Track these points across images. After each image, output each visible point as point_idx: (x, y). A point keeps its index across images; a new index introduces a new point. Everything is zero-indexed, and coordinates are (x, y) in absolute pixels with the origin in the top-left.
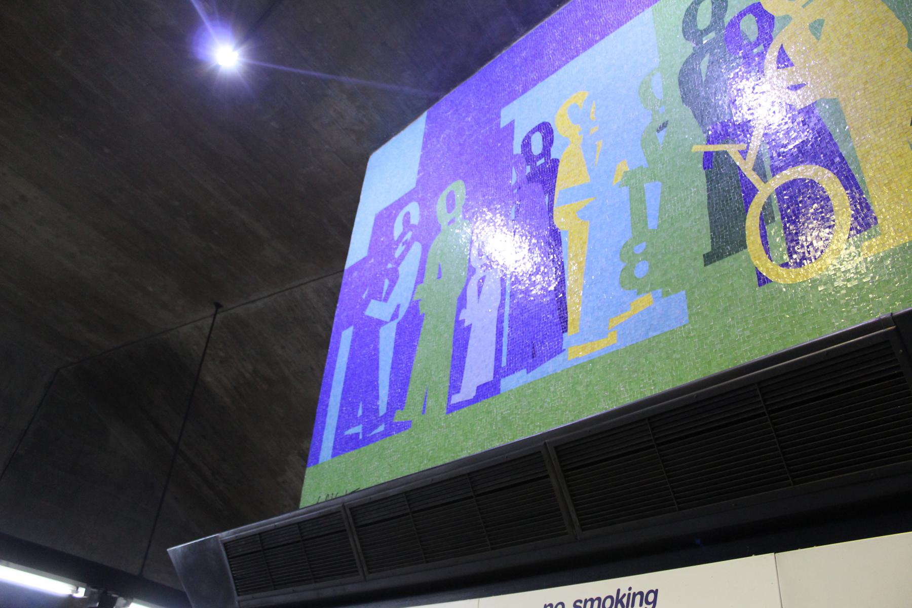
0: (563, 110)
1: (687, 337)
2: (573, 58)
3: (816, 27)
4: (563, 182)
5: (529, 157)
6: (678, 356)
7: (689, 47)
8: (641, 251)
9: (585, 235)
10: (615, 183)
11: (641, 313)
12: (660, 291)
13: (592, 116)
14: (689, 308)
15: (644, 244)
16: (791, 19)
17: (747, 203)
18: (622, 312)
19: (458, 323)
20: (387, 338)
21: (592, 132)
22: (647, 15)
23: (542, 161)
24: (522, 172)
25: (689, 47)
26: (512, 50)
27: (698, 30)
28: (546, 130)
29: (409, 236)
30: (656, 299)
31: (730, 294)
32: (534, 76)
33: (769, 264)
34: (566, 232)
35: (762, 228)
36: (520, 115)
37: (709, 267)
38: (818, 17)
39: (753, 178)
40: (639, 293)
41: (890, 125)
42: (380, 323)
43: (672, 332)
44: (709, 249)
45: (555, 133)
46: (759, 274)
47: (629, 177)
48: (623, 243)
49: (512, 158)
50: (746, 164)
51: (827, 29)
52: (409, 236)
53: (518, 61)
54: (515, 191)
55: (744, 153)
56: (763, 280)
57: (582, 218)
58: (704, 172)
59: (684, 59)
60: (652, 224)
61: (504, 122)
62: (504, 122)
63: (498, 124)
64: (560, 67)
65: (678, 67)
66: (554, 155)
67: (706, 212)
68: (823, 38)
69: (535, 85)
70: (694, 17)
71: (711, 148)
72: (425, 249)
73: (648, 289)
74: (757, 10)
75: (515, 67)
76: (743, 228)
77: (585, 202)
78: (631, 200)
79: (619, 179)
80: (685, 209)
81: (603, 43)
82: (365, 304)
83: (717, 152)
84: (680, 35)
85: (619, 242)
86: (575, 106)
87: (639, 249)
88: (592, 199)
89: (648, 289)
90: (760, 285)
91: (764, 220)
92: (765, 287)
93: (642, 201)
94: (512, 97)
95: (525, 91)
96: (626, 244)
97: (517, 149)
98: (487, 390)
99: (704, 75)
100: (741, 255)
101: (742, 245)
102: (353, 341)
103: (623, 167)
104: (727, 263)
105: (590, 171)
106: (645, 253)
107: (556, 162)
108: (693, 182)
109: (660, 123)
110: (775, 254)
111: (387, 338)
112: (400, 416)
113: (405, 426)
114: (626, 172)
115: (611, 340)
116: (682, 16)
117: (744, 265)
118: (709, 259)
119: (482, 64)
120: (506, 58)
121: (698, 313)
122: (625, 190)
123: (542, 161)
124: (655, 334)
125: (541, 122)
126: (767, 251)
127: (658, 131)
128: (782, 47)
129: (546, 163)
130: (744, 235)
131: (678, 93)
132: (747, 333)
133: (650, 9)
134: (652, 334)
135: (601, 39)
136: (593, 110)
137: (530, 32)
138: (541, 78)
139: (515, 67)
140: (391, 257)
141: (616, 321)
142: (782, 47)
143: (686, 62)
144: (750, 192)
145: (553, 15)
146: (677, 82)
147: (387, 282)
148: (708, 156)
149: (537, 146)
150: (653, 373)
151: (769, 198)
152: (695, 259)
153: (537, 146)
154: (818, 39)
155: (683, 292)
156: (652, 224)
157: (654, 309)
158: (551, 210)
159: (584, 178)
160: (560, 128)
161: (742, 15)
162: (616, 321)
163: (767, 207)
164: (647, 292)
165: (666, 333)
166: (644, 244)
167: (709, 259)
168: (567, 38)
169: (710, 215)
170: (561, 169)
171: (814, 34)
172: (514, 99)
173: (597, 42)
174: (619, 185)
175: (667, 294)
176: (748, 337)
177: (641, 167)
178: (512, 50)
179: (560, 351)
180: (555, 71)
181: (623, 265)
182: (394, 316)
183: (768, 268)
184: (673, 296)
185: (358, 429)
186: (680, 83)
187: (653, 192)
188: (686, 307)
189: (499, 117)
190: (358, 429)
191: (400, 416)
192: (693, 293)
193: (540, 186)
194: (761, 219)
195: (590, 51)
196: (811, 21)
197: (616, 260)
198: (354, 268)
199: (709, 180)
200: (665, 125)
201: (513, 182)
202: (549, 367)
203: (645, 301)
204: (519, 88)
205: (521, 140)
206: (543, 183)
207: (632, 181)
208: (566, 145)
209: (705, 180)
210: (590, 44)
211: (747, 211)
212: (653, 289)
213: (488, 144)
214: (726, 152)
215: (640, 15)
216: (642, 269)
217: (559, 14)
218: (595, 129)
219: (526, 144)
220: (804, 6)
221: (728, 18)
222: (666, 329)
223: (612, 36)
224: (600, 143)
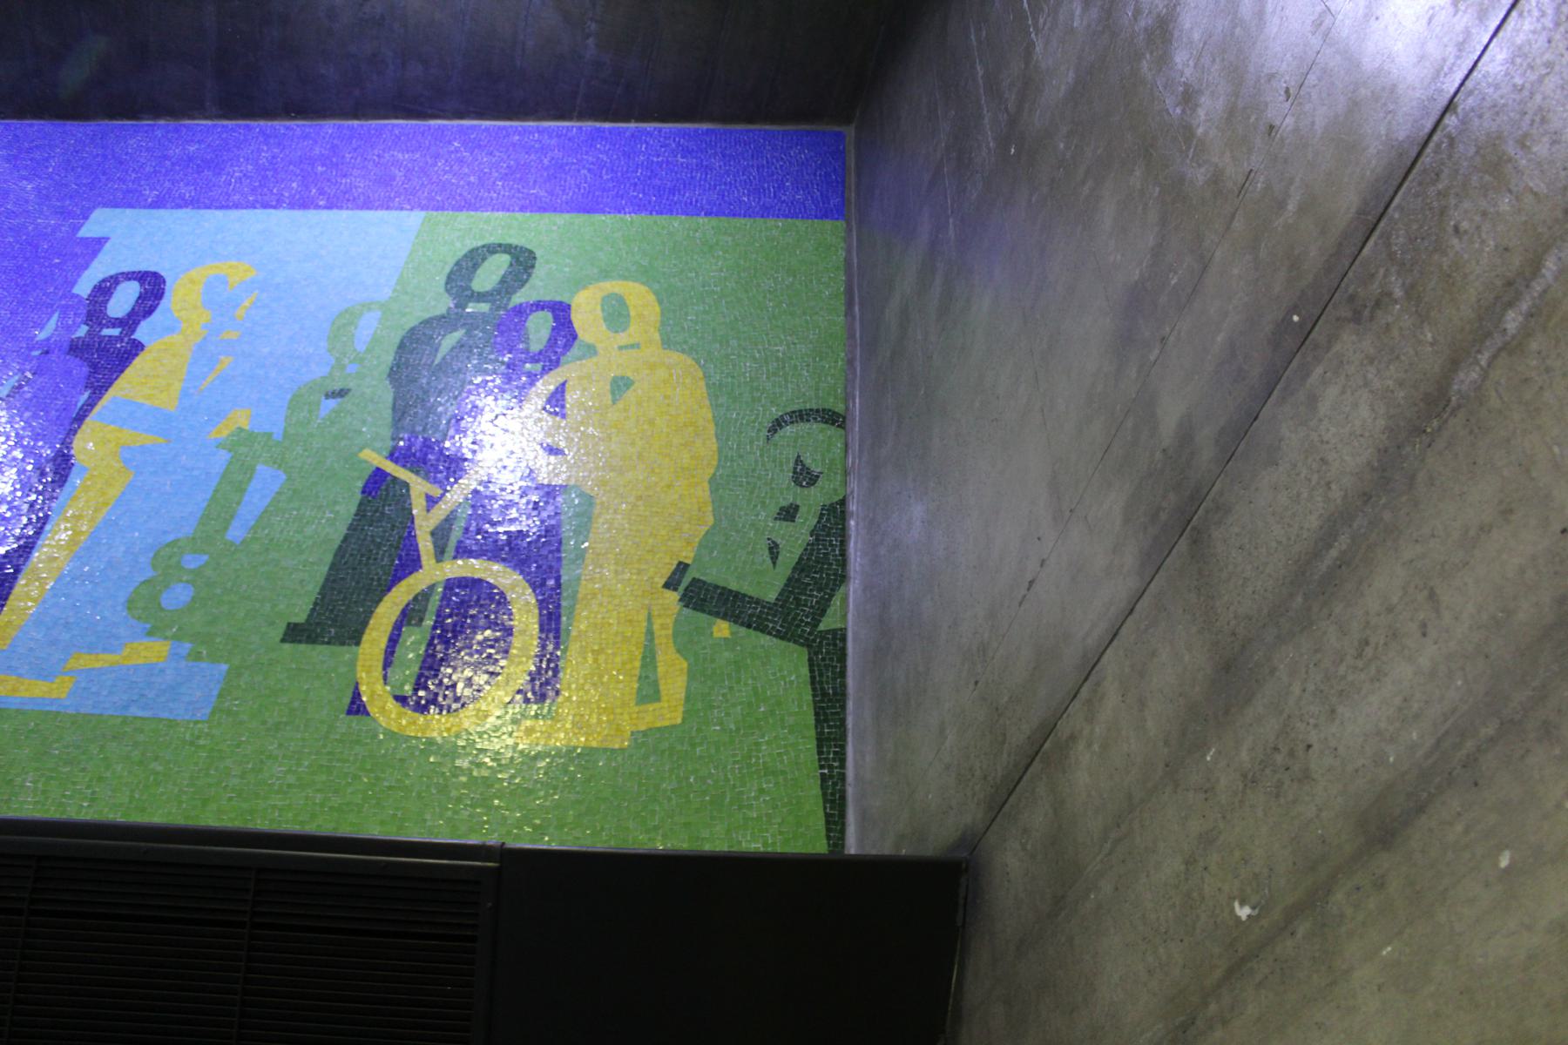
0: (200, 274)
1: (192, 743)
2: (266, 206)
3: (620, 385)
4: (129, 385)
6: (160, 768)
7: (443, 304)
8: (192, 567)
9: (114, 493)
10: (213, 435)
11: (136, 668)
12: (188, 645)
13: (240, 312)
14: (220, 696)
15: (205, 558)
16: (596, 353)
17: (396, 579)
18: (105, 650)
21: (225, 336)
22: (414, 219)
23: (116, 332)
24: (68, 329)
25: (443, 304)
26: (177, 130)
27: (469, 288)
28: (153, 288)
30: (174, 655)
31: (296, 704)
32: (187, 192)
33: (379, 687)
34: (85, 469)
35: (398, 627)
36: (126, 237)
37: (287, 646)
38: (629, 374)
39: (425, 545)
40: (150, 634)
41: (639, 572)
43: (172, 724)
44: (300, 617)
45: (164, 303)
46: (357, 695)
47: (243, 439)
48: (171, 537)
49: (64, 296)
50: (426, 519)
51: (630, 396)
53: (175, 151)
54: (36, 353)
55: (431, 501)
56: (357, 707)
57: (126, 462)
58: (359, 496)
59: (427, 316)
60: (236, 533)
61: (89, 230)
62: (89, 230)
63: (77, 228)
64: (237, 206)
65: (411, 322)
66: (140, 334)
67: (329, 558)
68: (620, 405)
69: (179, 207)
70: (476, 266)
71: (390, 467)
73: (169, 634)
74: (561, 312)
75: (166, 157)
76: (369, 613)
77: (147, 439)
78: (224, 476)
79: (223, 431)
80: (299, 537)
81: (325, 215)
83: (395, 478)
84: (441, 279)
85: (165, 532)
86: (223, 280)
87: (192, 562)
88: (161, 440)
89: (169, 634)
90: (349, 712)
91: (409, 616)
92: (355, 720)
93: (241, 490)
94: (129, 200)
95: (158, 204)
96: (176, 541)
97: (84, 287)
99: (439, 356)
100: (345, 653)
101: (356, 638)
103: (241, 419)
104: (318, 654)
105: (185, 394)
106: (198, 572)
107: (138, 347)
108: (335, 503)
109: (337, 386)
110: (395, 674)
114: (241, 430)
115: (55, 690)
116: (460, 254)
117: (342, 670)
118: (294, 633)
119: (112, 117)
120: (159, 133)
121: (229, 712)
122: (223, 456)
123: (116, 332)
124: (140, 713)
125: (152, 269)
126: (387, 664)
127: (327, 396)
128: (563, 384)
129: (119, 339)
130: (365, 623)
131: (389, 358)
132: (291, 779)
133: (423, 214)
134: (135, 711)
135: (329, 207)
136: (247, 303)
137: (225, 122)
138: (194, 203)
139: (166, 157)
141: (85, 661)
142: (563, 384)
143: (427, 322)
144: (411, 563)
145: (275, 123)
146: (397, 341)
148: (379, 476)
149: (122, 301)
150: (100, 779)
151: (432, 587)
152: (273, 623)
153: (122, 301)
154: (614, 402)
155: (225, 667)
156: (236, 533)
157: (162, 671)
158: (80, 418)
159: (168, 401)
160: (177, 297)
161: (539, 306)
162: (85, 661)
163: (422, 598)
164: (166, 638)
165: (161, 720)
166: (205, 558)
167: (294, 633)
168: (275, 170)
169: (333, 566)
170: (137, 361)
171: (613, 393)
172: (131, 206)
173: (318, 207)
174: (220, 445)
175: (198, 657)
176: (289, 786)
177: (270, 435)
178: (177, 130)
180: (227, 207)
181: (149, 574)
183: (375, 692)
184: (203, 665)
186: (401, 346)
187: (266, 483)
188: (215, 693)
189: (86, 218)
192: (239, 675)
193: (86, 370)
194: (404, 613)
195: (298, 214)
196: (619, 373)
197: (142, 559)
199: (361, 513)
200: (342, 393)
201: (41, 335)
203: (154, 651)
204: (151, 195)
205: (101, 276)
206: (95, 367)
207: (243, 450)
208: (171, 330)
209: (353, 509)
210: (304, 204)
211: (389, 590)
212: (177, 638)
213: (36, 247)
214: (406, 485)
215: (404, 213)
216: (178, 595)
217: (287, 128)
218: (232, 335)
219: (104, 289)
220: (621, 348)
221: (518, 298)
222: (165, 715)
223: (344, 214)
224: (226, 361)
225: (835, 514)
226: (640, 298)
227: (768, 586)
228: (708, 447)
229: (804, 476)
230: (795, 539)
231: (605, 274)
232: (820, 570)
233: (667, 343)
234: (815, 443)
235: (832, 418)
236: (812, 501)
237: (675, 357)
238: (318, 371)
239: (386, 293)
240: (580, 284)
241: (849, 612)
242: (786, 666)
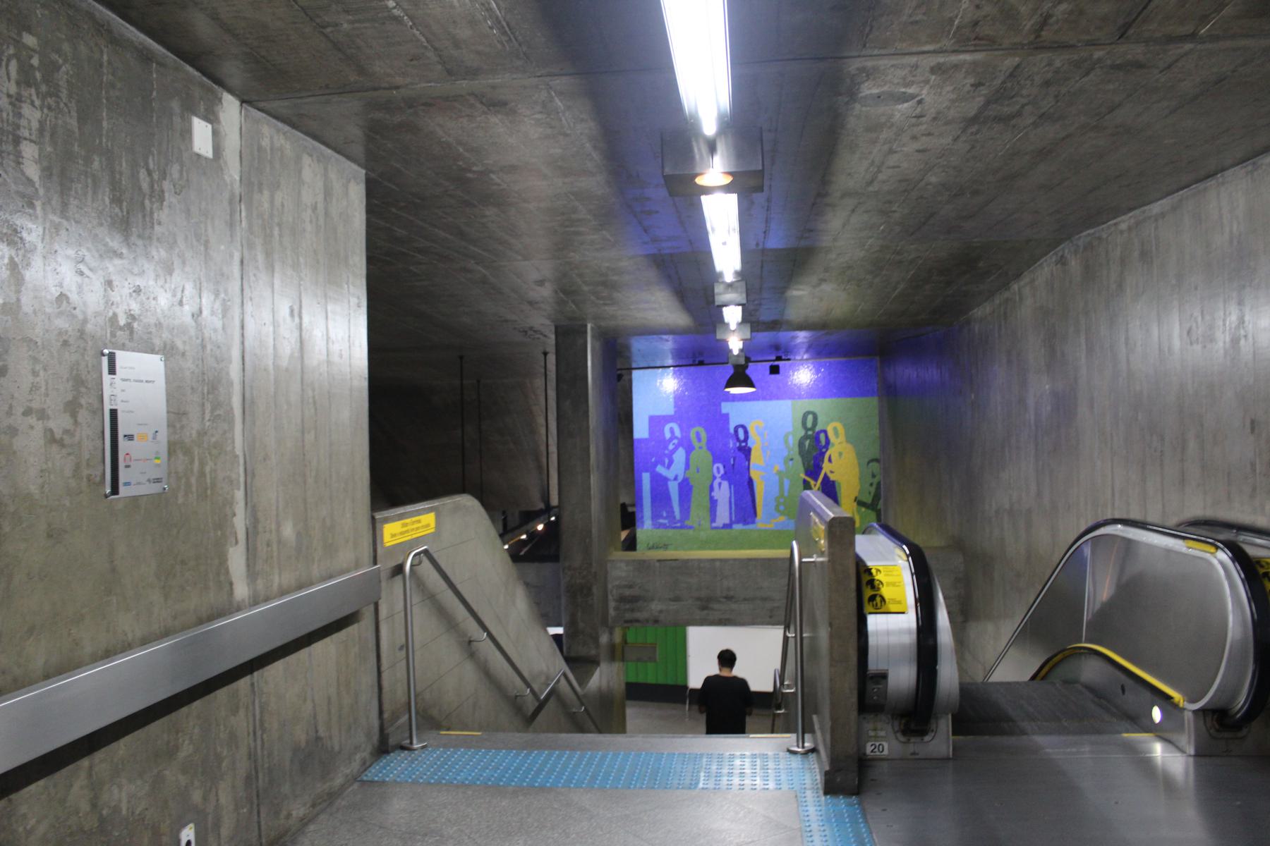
3: (840, 454)
5: (738, 439)
7: (802, 433)
19: (712, 498)
20: (673, 488)
22: (789, 402)
29: (675, 441)
42: (666, 480)
47: (779, 472)
52: (675, 441)
66: (750, 444)
72: (688, 453)
74: (825, 432)
82: (655, 465)
97: (732, 431)
98: (725, 526)
102: (652, 481)
103: (777, 468)
111: (673, 488)
112: (688, 523)
113: (691, 527)
115: (771, 526)
140: (666, 447)
147: (667, 461)
148: (805, 481)
158: (749, 468)
179: (753, 522)
182: (676, 479)
185: (666, 521)
187: (787, 483)
190: (666, 521)
191: (688, 523)
198: (640, 441)
202: (751, 526)
203: (782, 519)
216: (782, 508)
219: (736, 429)
221: (817, 429)
225: (879, 484)
226: (839, 426)
227: (868, 500)
228: (857, 470)
229: (874, 476)
230: (873, 490)
231: (832, 420)
232: (877, 497)
233: (848, 441)
234: (875, 465)
235: (877, 460)
236: (875, 481)
237: (850, 447)
238: (786, 454)
239: (791, 429)
240: (828, 423)
241: (880, 505)
242: (873, 515)
